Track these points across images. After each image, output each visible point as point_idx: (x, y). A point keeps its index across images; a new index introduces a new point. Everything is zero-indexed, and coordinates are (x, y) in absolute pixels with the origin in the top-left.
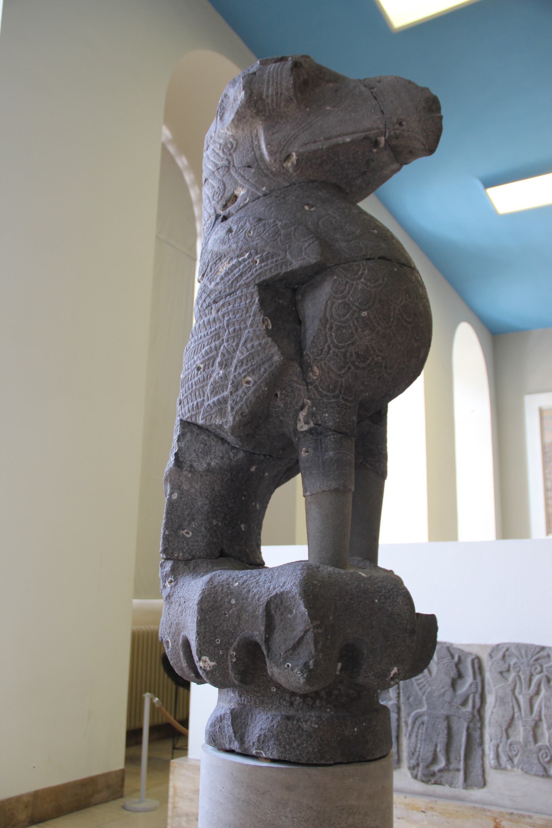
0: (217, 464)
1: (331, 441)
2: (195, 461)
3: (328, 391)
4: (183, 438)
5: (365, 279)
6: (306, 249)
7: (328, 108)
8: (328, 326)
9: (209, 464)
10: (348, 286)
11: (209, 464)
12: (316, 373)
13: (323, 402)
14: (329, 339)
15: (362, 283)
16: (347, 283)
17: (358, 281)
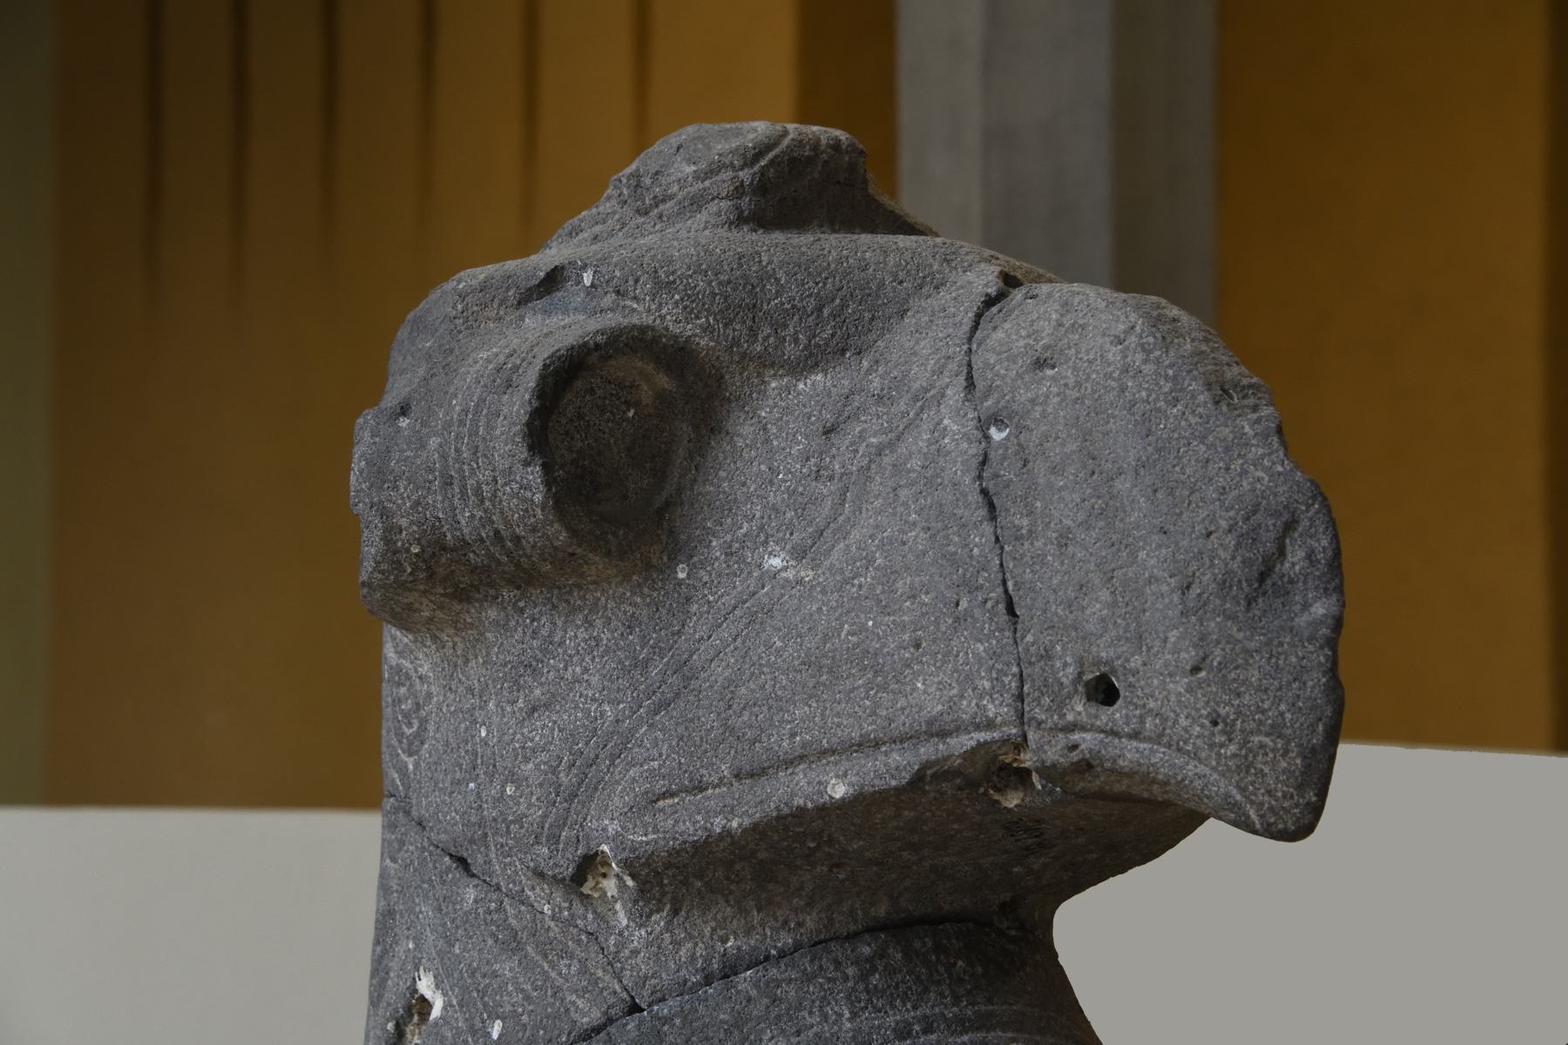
7: (776, 562)
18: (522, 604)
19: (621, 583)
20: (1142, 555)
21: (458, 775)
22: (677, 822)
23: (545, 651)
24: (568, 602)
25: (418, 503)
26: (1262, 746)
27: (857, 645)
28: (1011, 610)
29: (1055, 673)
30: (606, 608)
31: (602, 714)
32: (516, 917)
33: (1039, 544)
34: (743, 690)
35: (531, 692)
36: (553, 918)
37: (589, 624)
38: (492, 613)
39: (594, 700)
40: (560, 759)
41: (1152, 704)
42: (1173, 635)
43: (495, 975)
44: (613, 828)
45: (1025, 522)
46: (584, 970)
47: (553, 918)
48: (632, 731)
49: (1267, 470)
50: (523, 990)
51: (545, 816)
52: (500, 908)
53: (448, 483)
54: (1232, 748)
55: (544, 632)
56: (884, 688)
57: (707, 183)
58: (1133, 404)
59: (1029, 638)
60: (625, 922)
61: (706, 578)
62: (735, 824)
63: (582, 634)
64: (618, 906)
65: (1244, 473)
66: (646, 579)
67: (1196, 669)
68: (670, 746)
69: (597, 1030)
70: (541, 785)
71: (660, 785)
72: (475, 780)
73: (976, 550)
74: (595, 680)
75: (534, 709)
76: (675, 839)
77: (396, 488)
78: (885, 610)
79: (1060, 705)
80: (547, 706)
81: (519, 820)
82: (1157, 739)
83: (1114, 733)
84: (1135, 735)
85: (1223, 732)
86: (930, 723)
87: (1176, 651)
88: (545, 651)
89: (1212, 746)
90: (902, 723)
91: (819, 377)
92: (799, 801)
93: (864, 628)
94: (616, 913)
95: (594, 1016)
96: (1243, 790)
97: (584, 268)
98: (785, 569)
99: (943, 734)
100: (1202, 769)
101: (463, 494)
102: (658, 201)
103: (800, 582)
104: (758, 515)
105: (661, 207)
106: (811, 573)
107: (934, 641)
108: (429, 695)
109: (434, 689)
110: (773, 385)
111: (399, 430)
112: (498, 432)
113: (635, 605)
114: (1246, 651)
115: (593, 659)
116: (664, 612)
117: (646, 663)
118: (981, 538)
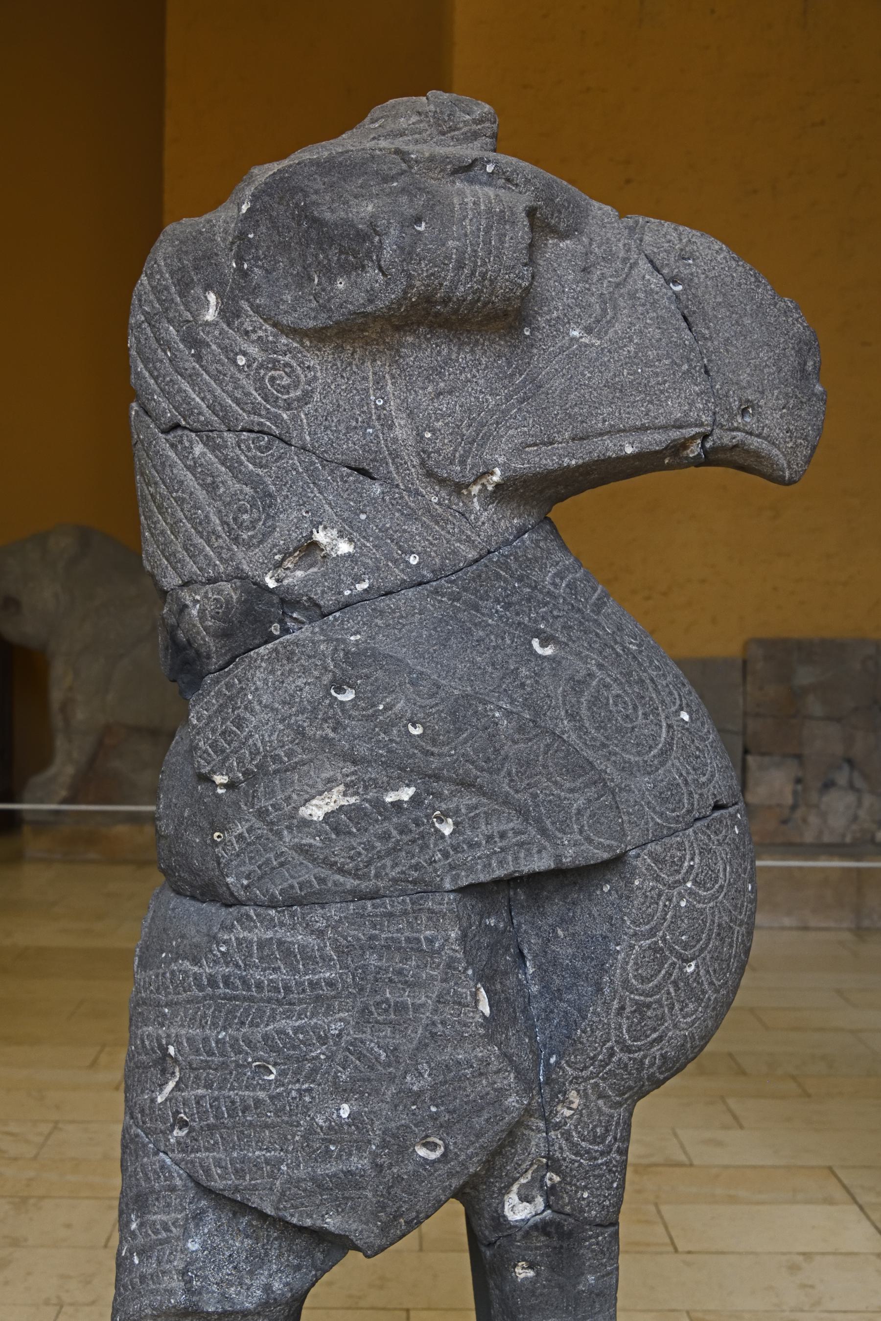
0: (287, 1284)
1: (593, 1251)
2: (230, 1284)
3: (594, 1142)
4: (197, 1226)
5: (695, 882)
6: (579, 812)
7: (575, 334)
8: (616, 1004)
9: (267, 1288)
10: (661, 903)
11: (267, 1288)
12: (572, 1102)
13: (581, 1164)
14: (613, 1033)
15: (691, 893)
16: (659, 895)
17: (681, 889)
18: (429, 336)
19: (494, 333)
20: (761, 355)
21: (354, 424)
22: (541, 459)
23: (446, 363)
24: (459, 339)
25: (432, 274)
26: (801, 444)
27: (635, 380)
28: (707, 372)
29: (730, 404)
30: (483, 344)
31: (487, 400)
32: (414, 502)
33: (716, 343)
34: (572, 396)
35: (438, 384)
36: (439, 503)
37: (472, 351)
38: (410, 339)
39: (481, 392)
40: (462, 421)
41: (767, 422)
42: (776, 392)
43: (405, 531)
44: (501, 460)
45: (707, 332)
46: (462, 532)
47: (439, 503)
48: (508, 410)
49: (801, 324)
50: (428, 540)
51: (455, 450)
52: (402, 498)
53: (460, 266)
54: (790, 445)
55: (445, 352)
56: (651, 402)
57: (479, 127)
58: (739, 285)
59: (718, 387)
60: (478, 508)
61: (540, 337)
62: (573, 462)
63: (469, 357)
64: (475, 500)
65: (794, 324)
66: (509, 333)
67: (783, 408)
68: (534, 421)
69: (476, 561)
70: (451, 434)
71: (530, 440)
72: (373, 427)
73: (687, 342)
74: (481, 382)
75: (441, 393)
76: (540, 468)
77: (419, 263)
78: (646, 365)
79: (732, 417)
80: (450, 393)
81: (438, 452)
82: (765, 438)
83: (751, 434)
84: (759, 436)
85: (790, 437)
86: (677, 420)
87: (778, 399)
88: (446, 363)
89: (785, 442)
90: (661, 421)
91: (568, 242)
92: (609, 454)
93: (636, 372)
94: (473, 503)
95: (472, 555)
96: (789, 462)
97: (489, 162)
98: (581, 337)
99: (680, 427)
100: (778, 452)
101: (473, 273)
102: (451, 129)
103: (593, 345)
104: (561, 308)
105: (453, 133)
106: (599, 342)
107: (674, 383)
108: (315, 378)
109: (319, 374)
110: (550, 242)
111: (419, 232)
112: (507, 245)
113: (500, 345)
114: (802, 402)
115: (478, 371)
116: (519, 351)
117: (512, 375)
118: (687, 335)
